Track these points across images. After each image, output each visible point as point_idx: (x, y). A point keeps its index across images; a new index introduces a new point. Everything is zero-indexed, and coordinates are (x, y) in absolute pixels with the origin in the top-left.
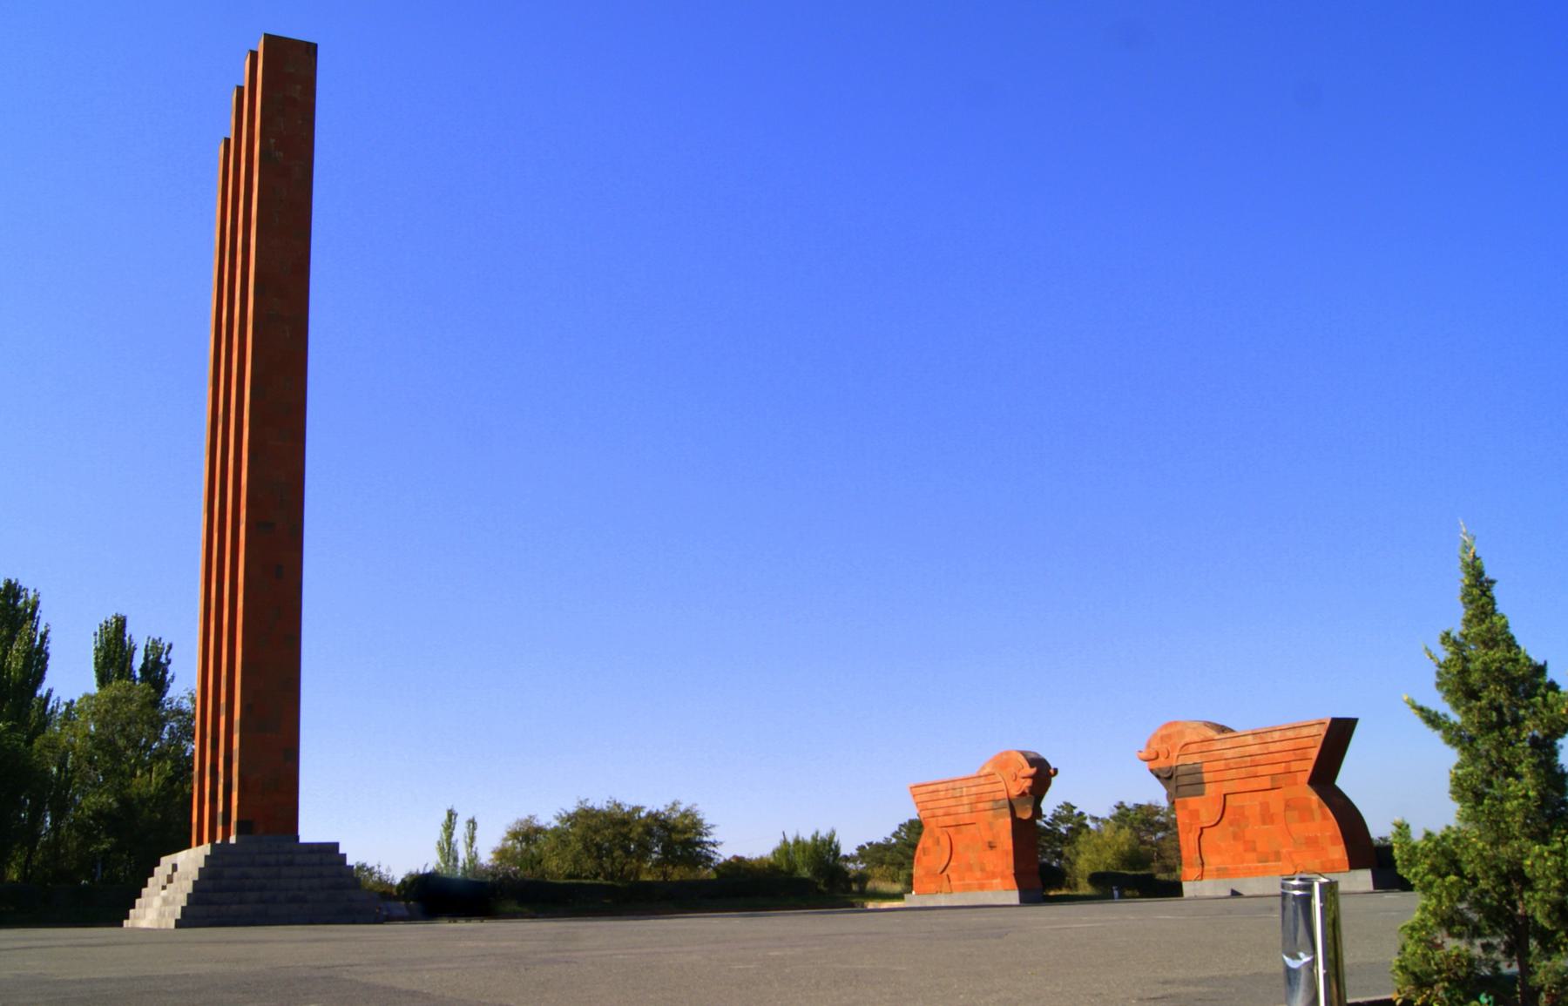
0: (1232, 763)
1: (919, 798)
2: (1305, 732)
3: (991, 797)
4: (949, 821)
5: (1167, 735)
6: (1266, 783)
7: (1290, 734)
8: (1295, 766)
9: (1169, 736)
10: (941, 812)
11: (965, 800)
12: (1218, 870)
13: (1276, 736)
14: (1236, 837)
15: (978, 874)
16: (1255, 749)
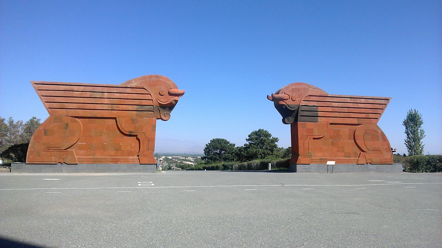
0: (337, 110)
1: (44, 93)
2: (378, 102)
3: (137, 102)
4: (81, 113)
5: (297, 88)
6: (355, 121)
7: (371, 101)
8: (371, 116)
9: (298, 90)
10: (75, 106)
11: (106, 101)
12: (321, 159)
13: (363, 101)
14: (333, 144)
15: (113, 153)
16: (351, 105)
